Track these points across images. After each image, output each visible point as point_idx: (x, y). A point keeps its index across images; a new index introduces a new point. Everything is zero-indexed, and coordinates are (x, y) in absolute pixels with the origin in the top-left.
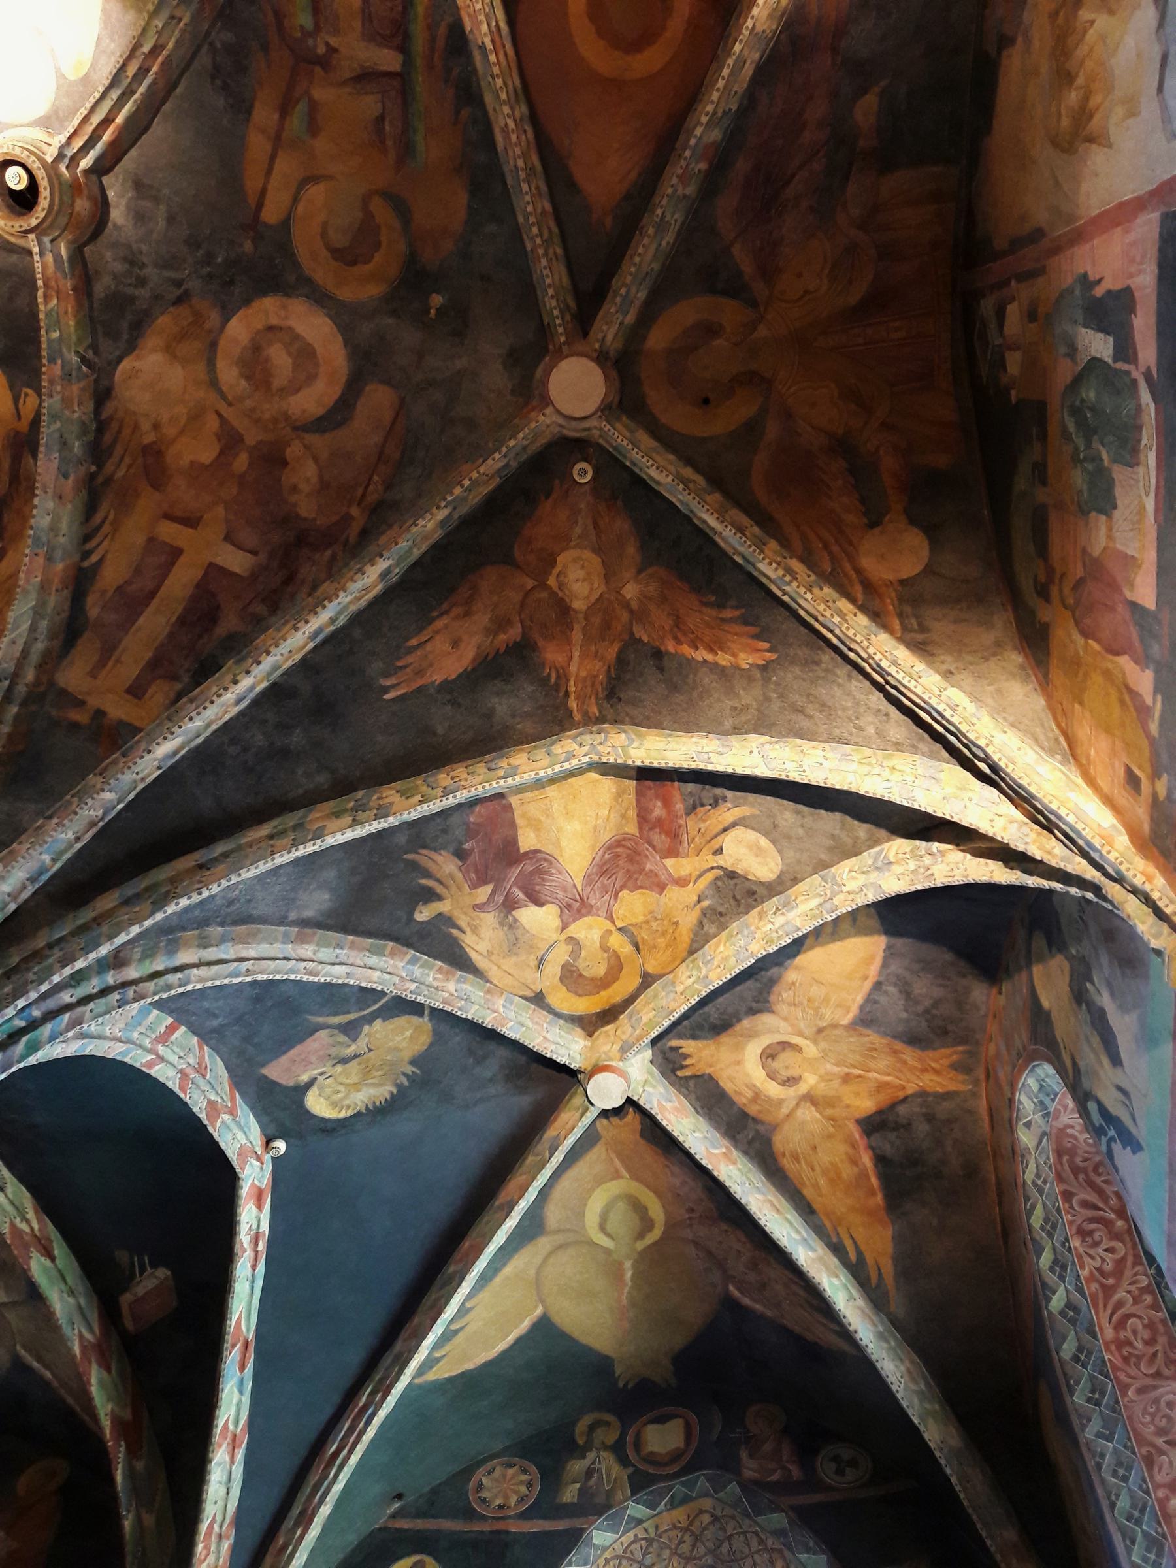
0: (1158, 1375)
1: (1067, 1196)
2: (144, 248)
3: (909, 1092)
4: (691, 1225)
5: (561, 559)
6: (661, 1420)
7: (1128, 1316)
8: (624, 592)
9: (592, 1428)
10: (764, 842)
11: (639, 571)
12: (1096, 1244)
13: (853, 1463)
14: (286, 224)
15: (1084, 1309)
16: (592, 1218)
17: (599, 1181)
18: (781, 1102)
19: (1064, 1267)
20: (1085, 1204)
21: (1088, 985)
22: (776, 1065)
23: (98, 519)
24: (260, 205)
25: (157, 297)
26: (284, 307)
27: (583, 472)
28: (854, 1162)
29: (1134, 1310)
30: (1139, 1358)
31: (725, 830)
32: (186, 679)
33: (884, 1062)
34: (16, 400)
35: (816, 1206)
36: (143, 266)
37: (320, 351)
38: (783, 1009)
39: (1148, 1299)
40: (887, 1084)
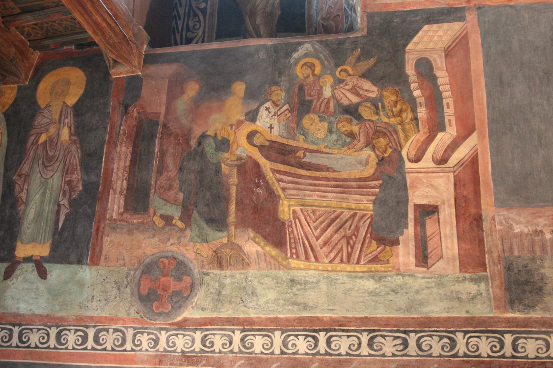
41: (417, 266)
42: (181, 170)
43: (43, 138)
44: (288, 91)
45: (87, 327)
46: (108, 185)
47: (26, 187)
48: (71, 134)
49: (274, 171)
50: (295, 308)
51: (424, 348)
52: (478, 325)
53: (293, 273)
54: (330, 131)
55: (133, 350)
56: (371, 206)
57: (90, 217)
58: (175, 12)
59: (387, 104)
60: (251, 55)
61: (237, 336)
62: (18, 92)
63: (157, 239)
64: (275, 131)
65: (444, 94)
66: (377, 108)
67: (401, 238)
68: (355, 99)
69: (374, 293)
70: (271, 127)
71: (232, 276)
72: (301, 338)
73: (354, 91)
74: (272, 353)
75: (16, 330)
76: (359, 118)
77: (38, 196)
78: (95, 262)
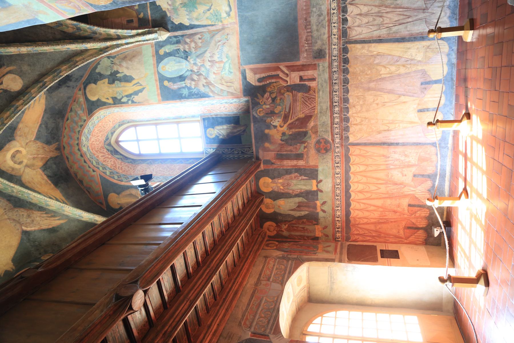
0: (134, 169)
3: (49, 158)
4: (6, 214)
7: (121, 168)
12: (108, 161)
15: (113, 171)
18: (20, 169)
19: (105, 168)
20: (102, 156)
21: (117, 75)
22: (15, 159)
28: (43, 179)
33: (41, 151)
35: (40, 192)
38: (18, 138)
39: (123, 163)
40: (43, 158)
41: (316, 81)
42: (291, 145)
43: (282, 188)
44: (268, 117)
45: (335, 166)
46: (296, 166)
47: (296, 190)
48: (280, 179)
49: (291, 119)
50: (327, 111)
51: (336, 79)
52: (330, 65)
53: (318, 113)
54: (279, 105)
55: (340, 153)
56: (300, 93)
57: (305, 169)
58: (232, 158)
59: (271, 90)
60: (257, 129)
61: (335, 126)
62: (267, 198)
63: (310, 150)
64: (279, 120)
65: (268, 75)
66: (273, 93)
67: (309, 85)
68: (270, 99)
69: (323, 92)
70: (278, 121)
71: (320, 128)
72: (335, 109)
73: (267, 99)
74: (339, 116)
75: (336, 186)
76: (276, 97)
77: (299, 186)
78: (317, 166)
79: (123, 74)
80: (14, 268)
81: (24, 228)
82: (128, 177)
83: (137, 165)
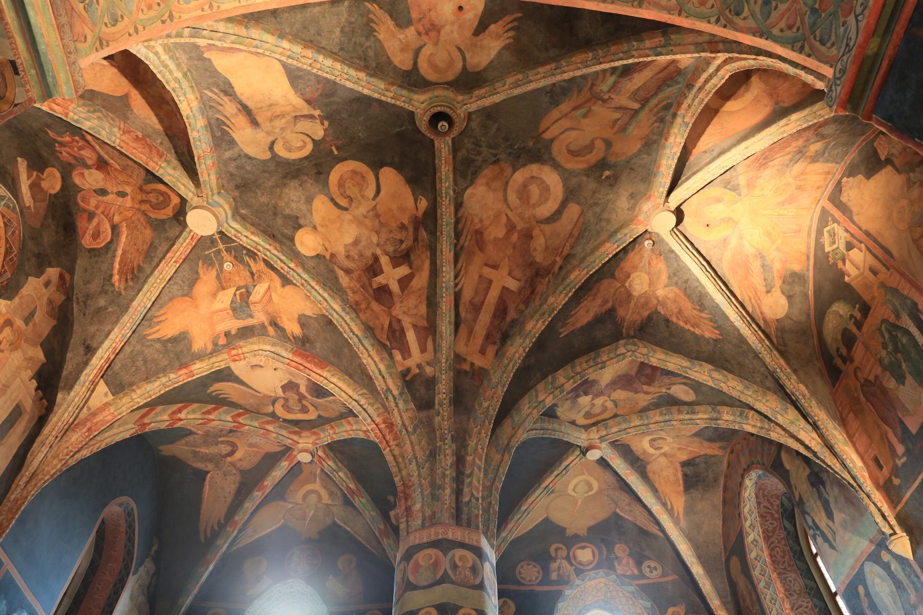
0: (785, 569)
1: (759, 504)
2: (483, 139)
5: (632, 276)
6: (582, 548)
8: (656, 292)
9: (557, 550)
10: (691, 391)
11: (666, 286)
12: (767, 521)
13: (655, 568)
14: (552, 140)
16: (571, 486)
17: (576, 476)
18: (653, 455)
19: (754, 527)
20: (765, 507)
22: (655, 443)
23: (459, 265)
24: (544, 132)
25: (485, 161)
26: (540, 169)
27: (648, 244)
28: (675, 475)
29: (777, 545)
30: (779, 562)
31: (674, 384)
32: (498, 343)
34: (416, 201)
36: (481, 146)
37: (552, 188)
39: (783, 542)
40: (694, 452)
79: (827, 496)
80: (586, 535)
81: (618, 510)
82: (765, 572)
83: (795, 567)
